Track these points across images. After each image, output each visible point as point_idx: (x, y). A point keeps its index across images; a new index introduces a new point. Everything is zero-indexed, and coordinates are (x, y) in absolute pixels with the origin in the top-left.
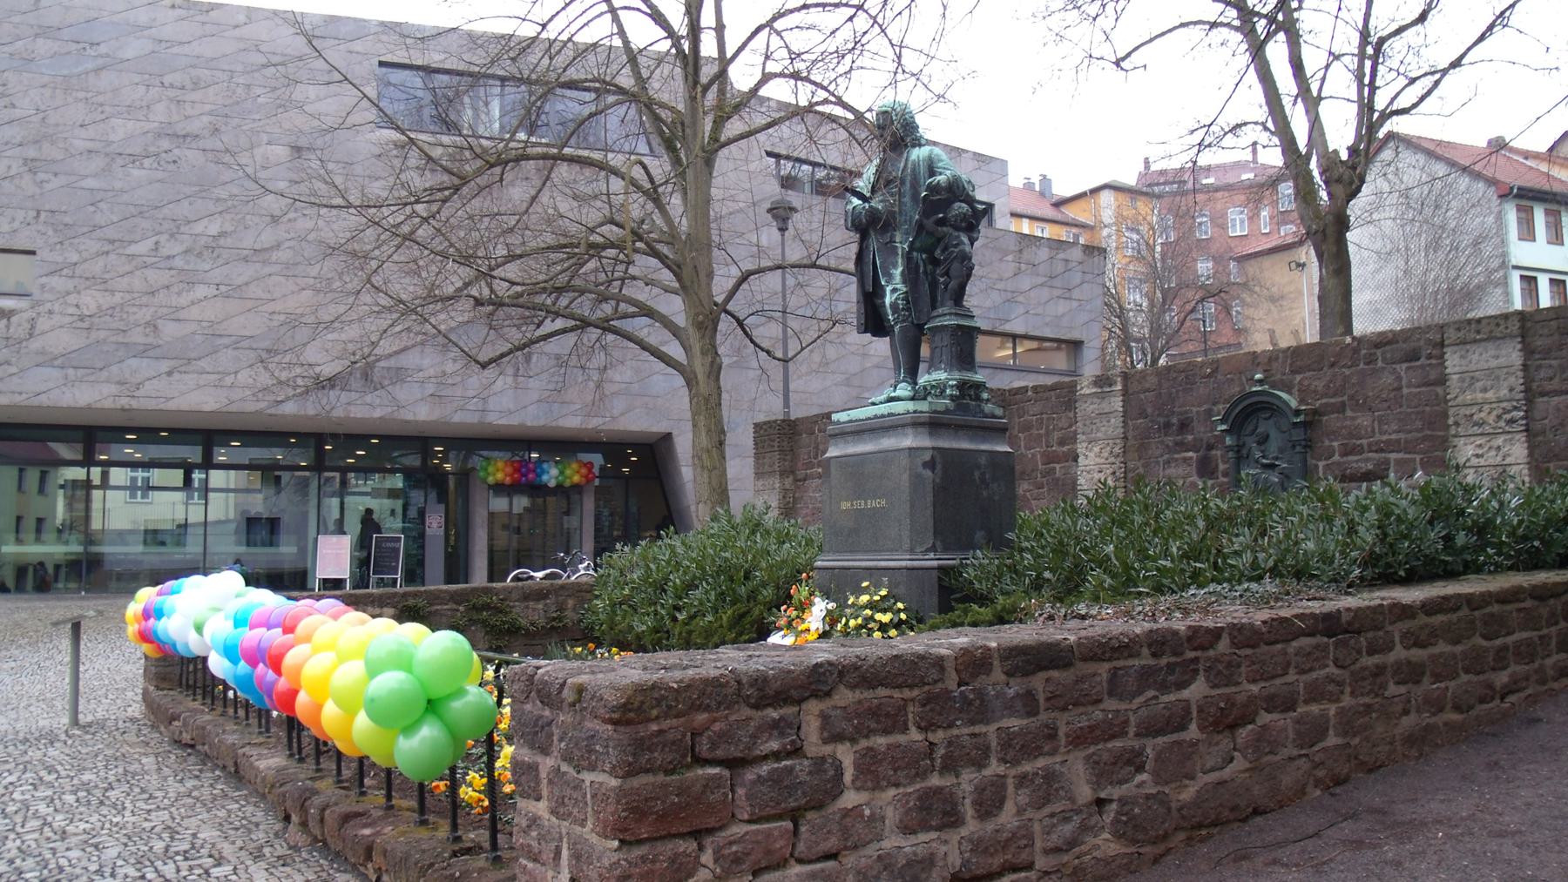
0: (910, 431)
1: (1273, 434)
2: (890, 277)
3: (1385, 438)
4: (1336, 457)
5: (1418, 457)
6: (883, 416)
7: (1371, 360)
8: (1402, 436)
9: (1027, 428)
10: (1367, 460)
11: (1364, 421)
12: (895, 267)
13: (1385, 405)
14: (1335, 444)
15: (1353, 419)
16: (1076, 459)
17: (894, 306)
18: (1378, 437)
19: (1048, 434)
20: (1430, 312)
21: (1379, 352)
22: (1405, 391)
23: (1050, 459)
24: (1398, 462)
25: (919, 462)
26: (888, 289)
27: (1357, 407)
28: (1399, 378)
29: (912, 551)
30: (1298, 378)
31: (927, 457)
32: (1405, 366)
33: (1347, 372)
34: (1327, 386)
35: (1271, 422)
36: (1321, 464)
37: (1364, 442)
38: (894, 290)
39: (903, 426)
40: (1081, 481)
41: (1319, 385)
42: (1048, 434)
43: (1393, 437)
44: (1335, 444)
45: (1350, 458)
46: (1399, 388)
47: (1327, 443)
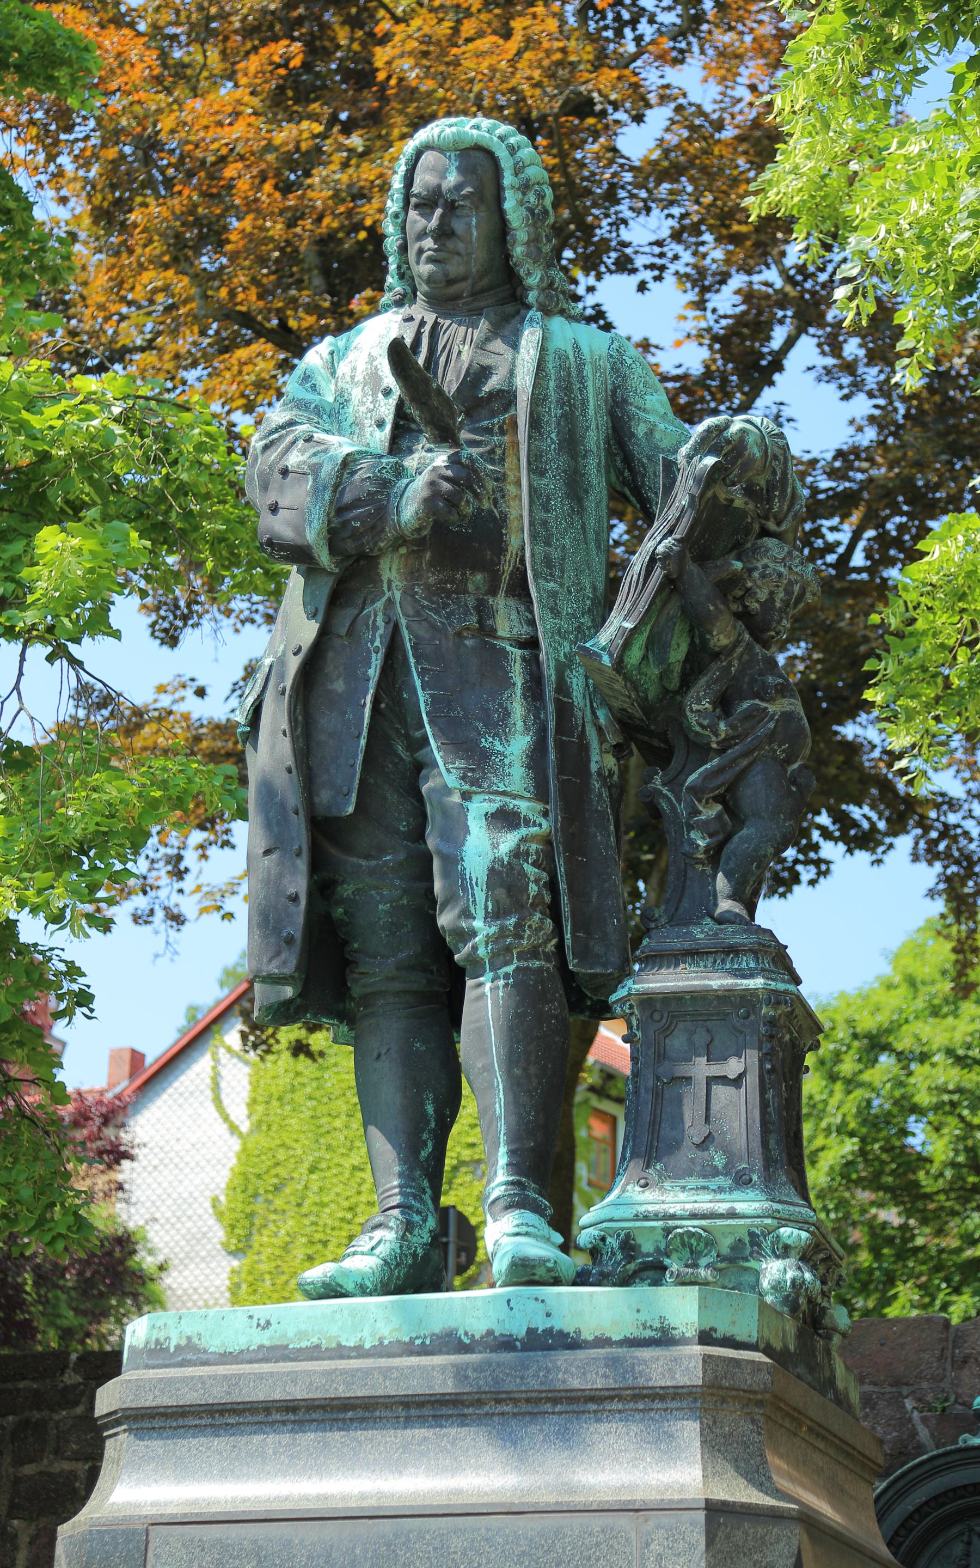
2: (480, 766)
12: (499, 724)
17: (504, 877)
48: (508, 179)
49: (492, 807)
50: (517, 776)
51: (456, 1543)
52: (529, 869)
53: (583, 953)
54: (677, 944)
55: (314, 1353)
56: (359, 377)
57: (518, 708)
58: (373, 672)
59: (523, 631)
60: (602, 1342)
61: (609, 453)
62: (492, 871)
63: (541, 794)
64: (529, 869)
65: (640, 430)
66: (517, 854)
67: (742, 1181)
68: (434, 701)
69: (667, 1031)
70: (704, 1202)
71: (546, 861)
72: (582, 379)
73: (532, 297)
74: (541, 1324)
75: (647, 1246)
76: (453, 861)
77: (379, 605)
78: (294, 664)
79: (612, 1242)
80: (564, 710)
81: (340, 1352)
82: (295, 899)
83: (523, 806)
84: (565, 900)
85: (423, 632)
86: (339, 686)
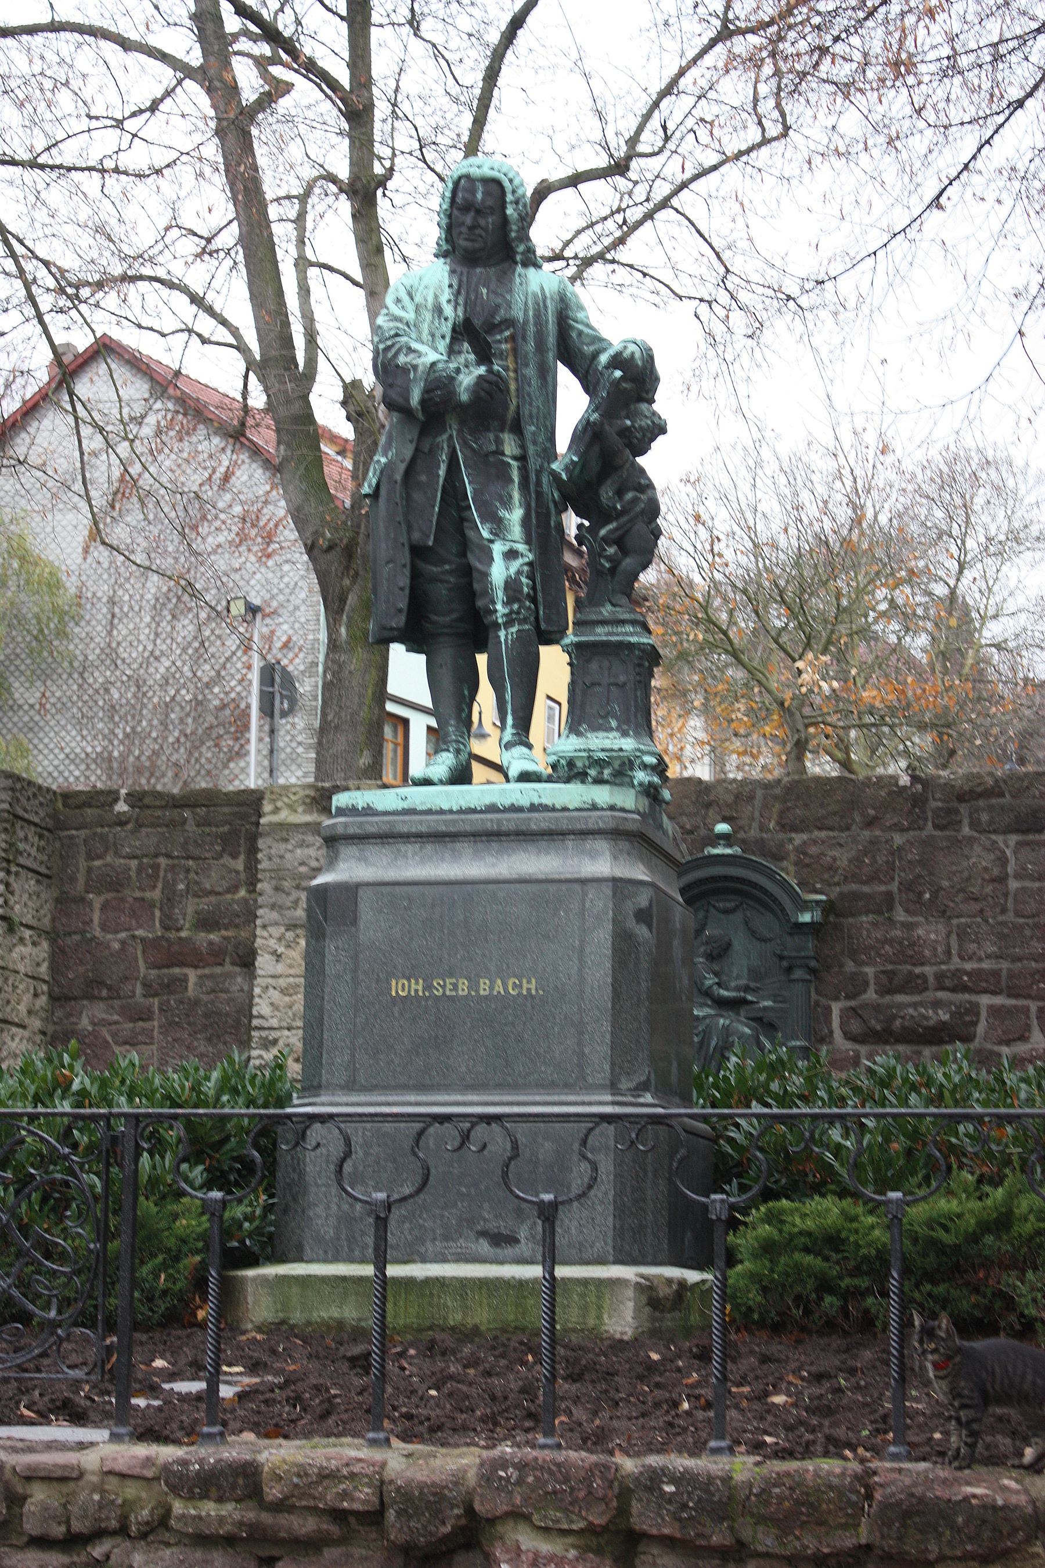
0: (602, 845)
1: (740, 942)
2: (499, 527)
3: (969, 966)
4: (871, 995)
5: (1033, 1006)
6: (514, 809)
7: (947, 820)
8: (1005, 965)
9: (114, 883)
10: (936, 1004)
11: (931, 932)
12: (507, 504)
13: (975, 907)
14: (870, 971)
15: (909, 926)
16: (247, 960)
17: (511, 586)
18: (956, 963)
19: (170, 898)
20: (149, 746)
21: (964, 809)
22: (1013, 885)
23: (173, 955)
24: (995, 1011)
25: (629, 907)
26: (498, 549)
27: (917, 905)
28: (1003, 861)
29: (613, 1087)
30: (799, 838)
31: (643, 899)
32: (1013, 839)
33: (898, 839)
34: (857, 861)
35: (738, 917)
36: (836, 1008)
37: (928, 970)
38: (511, 555)
39: (584, 834)
40: (262, 1007)
41: (842, 858)
42: (170, 898)
43: (986, 965)
44: (870, 971)
45: (900, 998)
46: (1002, 879)
47: (850, 966)
48: (509, 197)
49: (506, 548)
50: (516, 531)
51: (501, 895)
52: (524, 580)
53: (548, 620)
54: (594, 617)
55: (429, 812)
56: (430, 305)
57: (516, 495)
58: (442, 472)
59: (517, 452)
60: (565, 809)
61: (559, 346)
62: (506, 583)
63: (528, 541)
64: (524, 580)
65: (574, 335)
66: (519, 573)
67: (625, 734)
68: (475, 492)
69: (588, 661)
70: (607, 744)
71: (531, 577)
72: (545, 307)
73: (518, 258)
74: (536, 801)
75: (579, 764)
76: (486, 575)
77: (445, 437)
78: (402, 467)
79: (563, 762)
80: (539, 494)
81: (442, 812)
82: (402, 589)
83: (521, 547)
84: (540, 595)
85: (468, 453)
86: (423, 478)
